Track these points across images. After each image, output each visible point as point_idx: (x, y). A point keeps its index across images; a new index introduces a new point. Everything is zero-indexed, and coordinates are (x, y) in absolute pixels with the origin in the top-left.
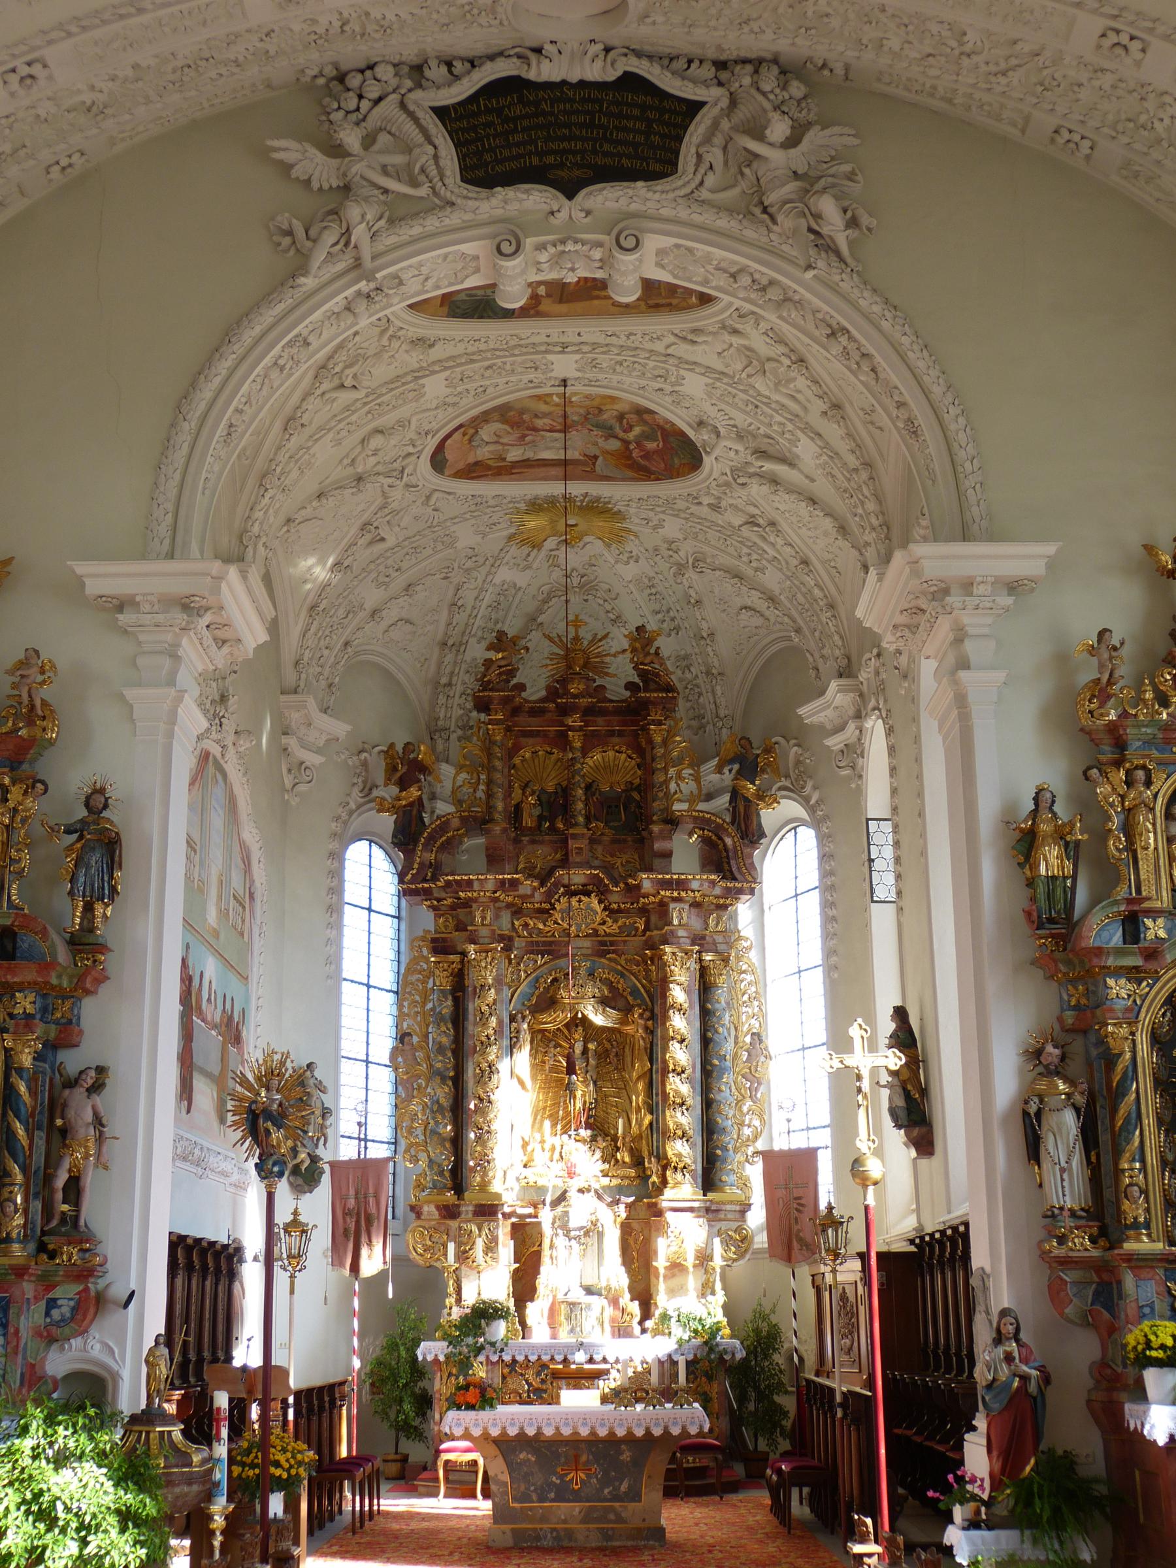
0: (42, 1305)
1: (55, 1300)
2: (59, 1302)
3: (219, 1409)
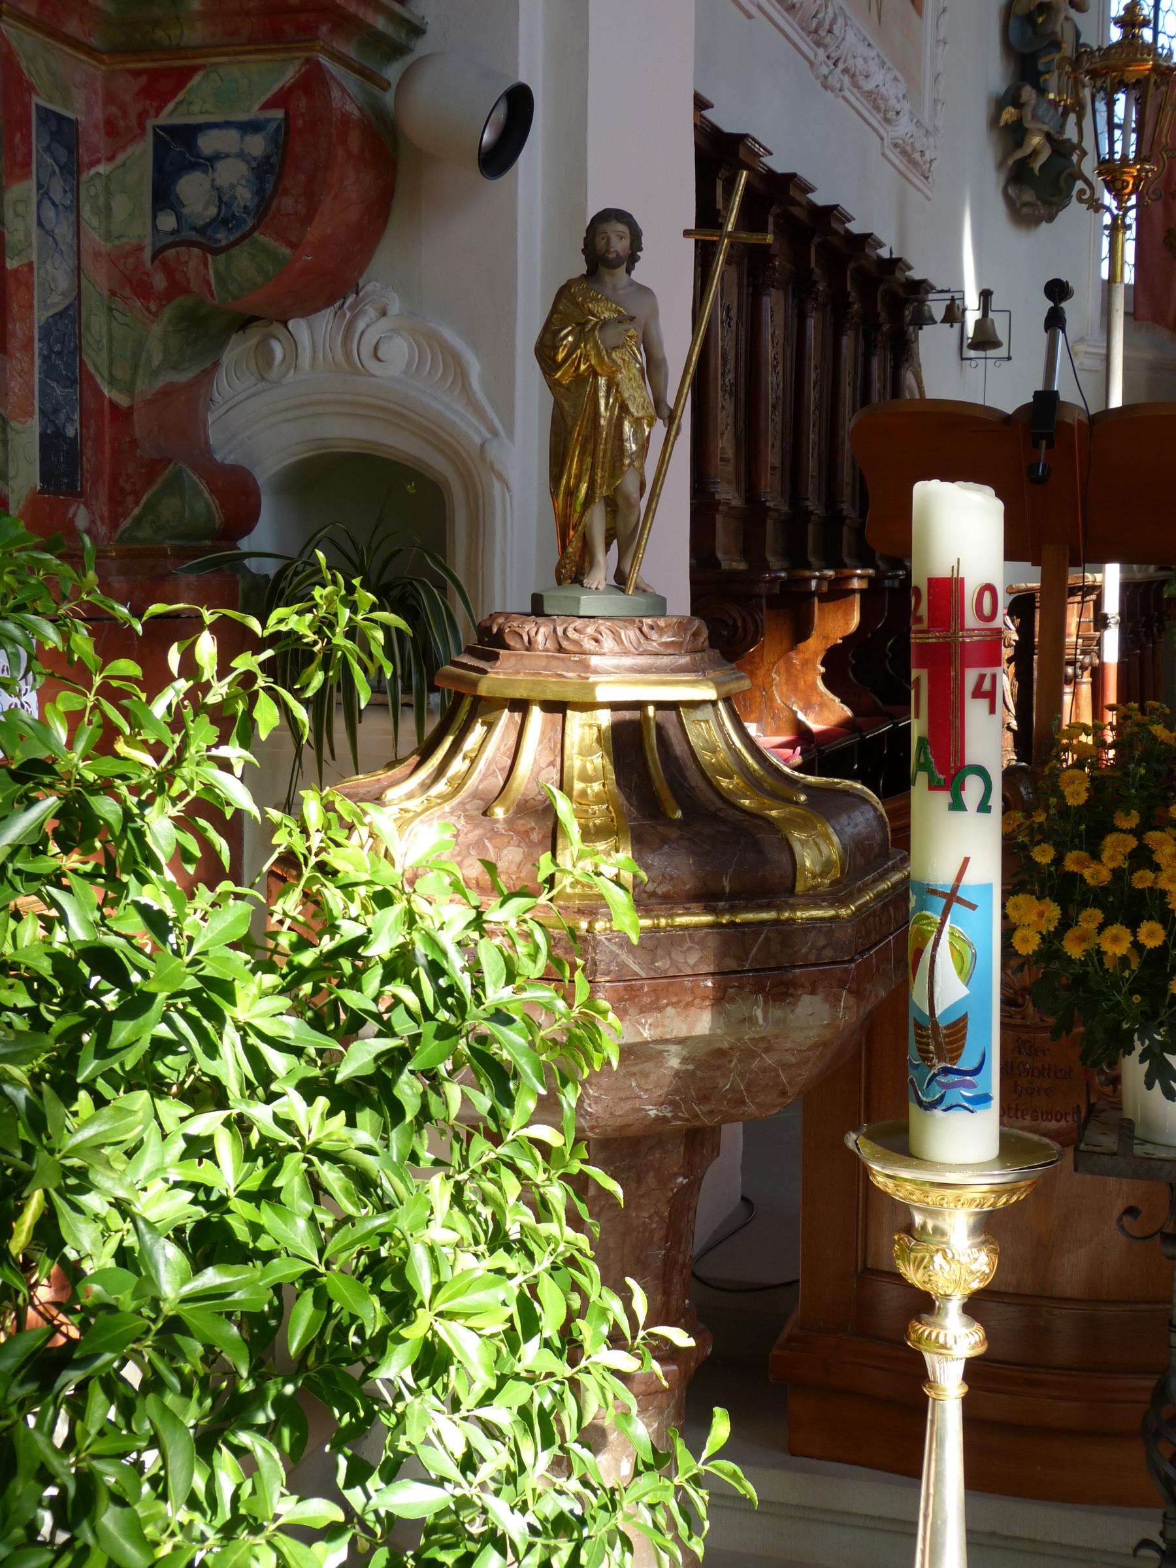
0: (141, 152)
1: (187, 134)
2: (207, 143)
3: (947, 590)
